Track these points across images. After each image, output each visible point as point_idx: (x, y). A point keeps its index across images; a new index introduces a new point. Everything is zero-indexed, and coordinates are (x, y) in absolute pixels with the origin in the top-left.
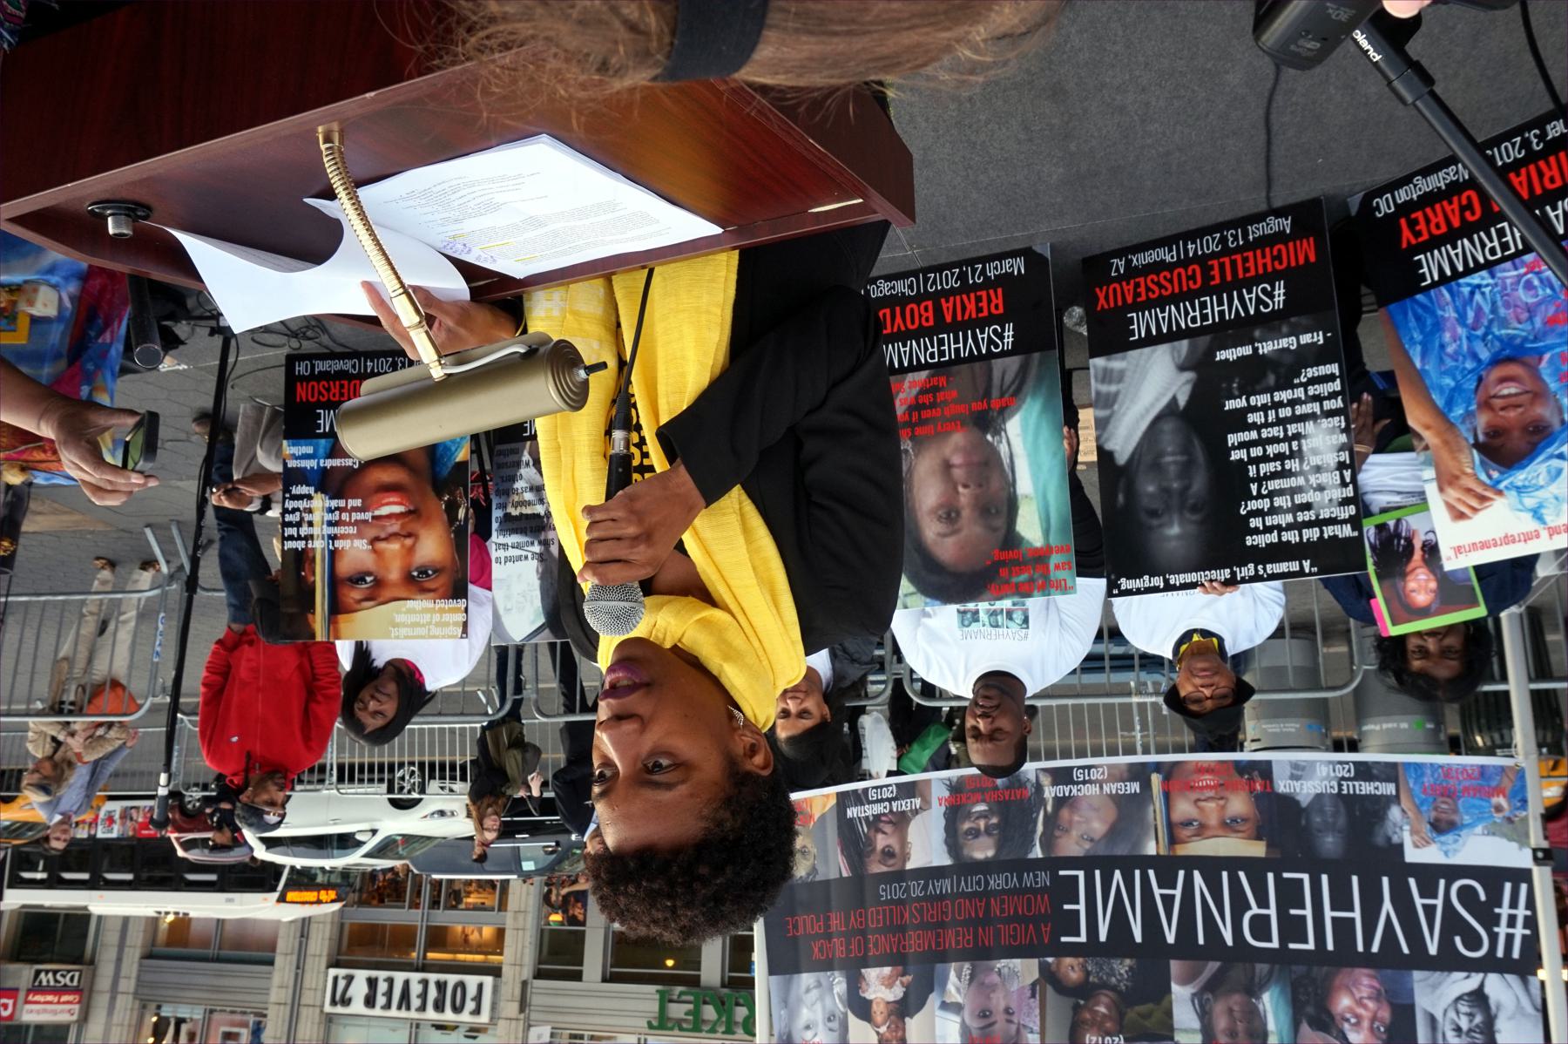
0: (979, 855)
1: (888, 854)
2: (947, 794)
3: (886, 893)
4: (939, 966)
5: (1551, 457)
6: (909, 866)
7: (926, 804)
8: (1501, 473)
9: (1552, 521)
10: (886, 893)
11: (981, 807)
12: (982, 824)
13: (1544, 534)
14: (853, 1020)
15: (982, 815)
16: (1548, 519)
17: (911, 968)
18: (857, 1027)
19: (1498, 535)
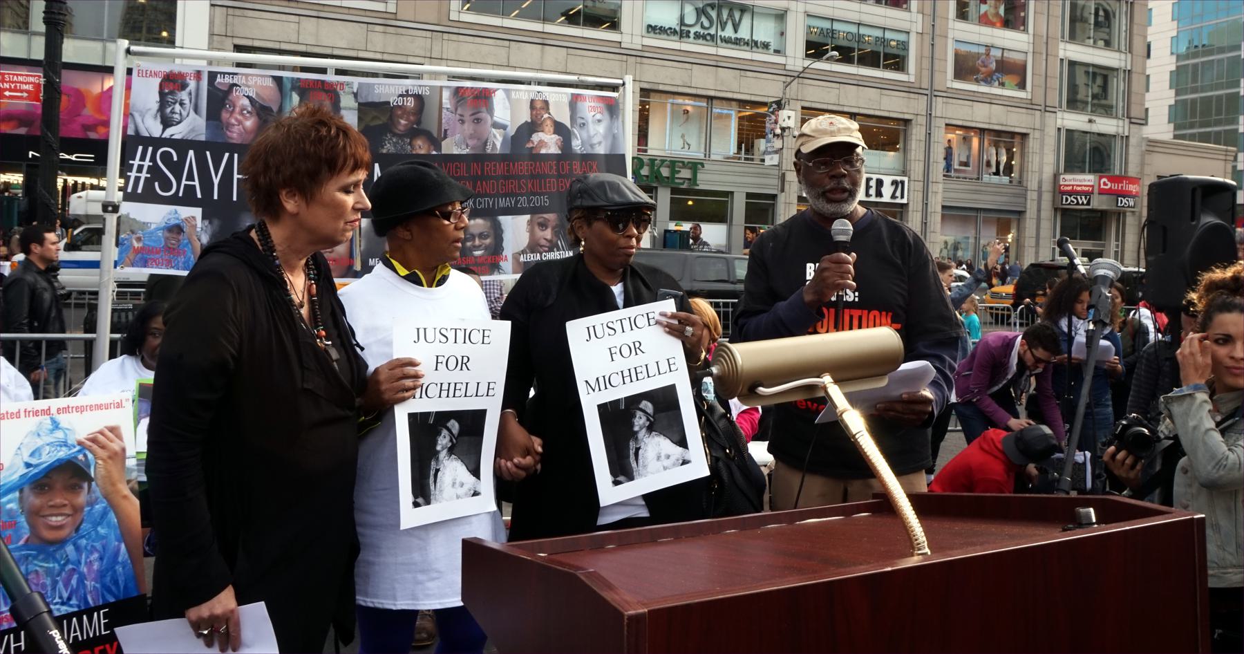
0: (479, 221)
1: (543, 226)
2: (501, 263)
3: (545, 200)
4: (508, 152)
5: (37, 466)
6: (528, 217)
7: (516, 257)
8: (76, 458)
9: (46, 420)
10: (545, 200)
11: (478, 253)
12: (477, 242)
13: (53, 411)
14: (567, 122)
15: (478, 248)
16: (49, 421)
17: (526, 152)
18: (565, 120)
19: (86, 414)
